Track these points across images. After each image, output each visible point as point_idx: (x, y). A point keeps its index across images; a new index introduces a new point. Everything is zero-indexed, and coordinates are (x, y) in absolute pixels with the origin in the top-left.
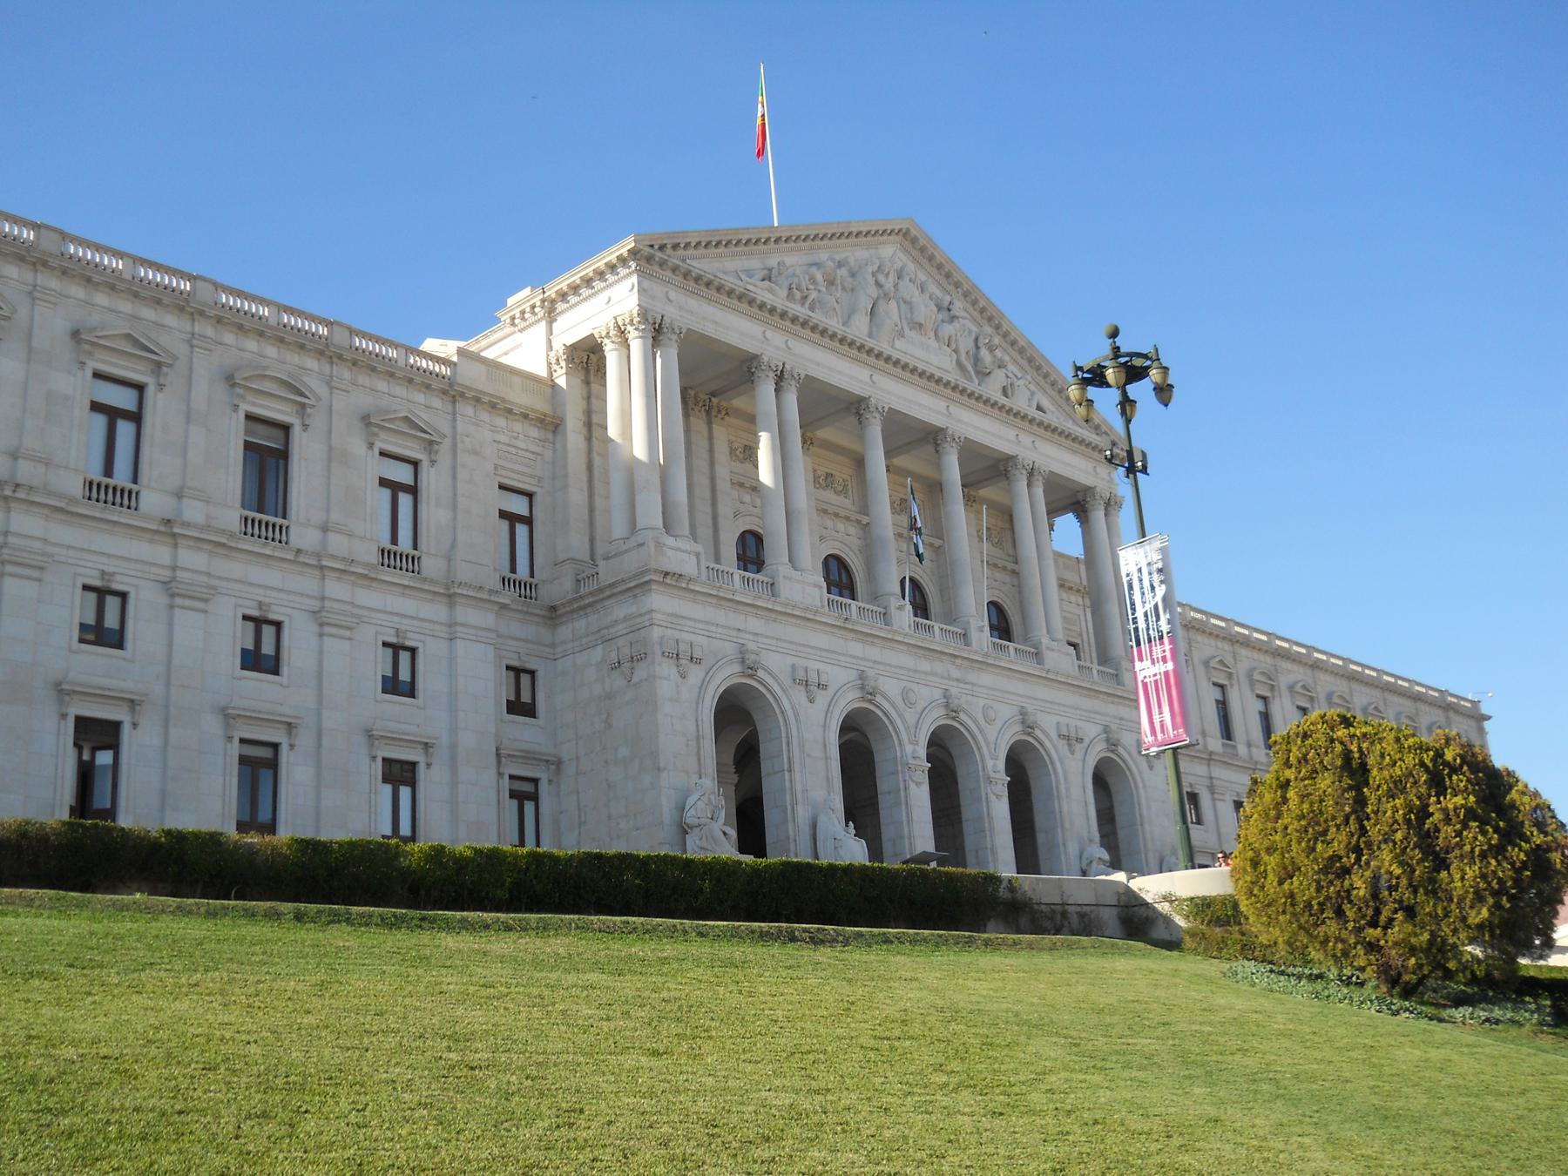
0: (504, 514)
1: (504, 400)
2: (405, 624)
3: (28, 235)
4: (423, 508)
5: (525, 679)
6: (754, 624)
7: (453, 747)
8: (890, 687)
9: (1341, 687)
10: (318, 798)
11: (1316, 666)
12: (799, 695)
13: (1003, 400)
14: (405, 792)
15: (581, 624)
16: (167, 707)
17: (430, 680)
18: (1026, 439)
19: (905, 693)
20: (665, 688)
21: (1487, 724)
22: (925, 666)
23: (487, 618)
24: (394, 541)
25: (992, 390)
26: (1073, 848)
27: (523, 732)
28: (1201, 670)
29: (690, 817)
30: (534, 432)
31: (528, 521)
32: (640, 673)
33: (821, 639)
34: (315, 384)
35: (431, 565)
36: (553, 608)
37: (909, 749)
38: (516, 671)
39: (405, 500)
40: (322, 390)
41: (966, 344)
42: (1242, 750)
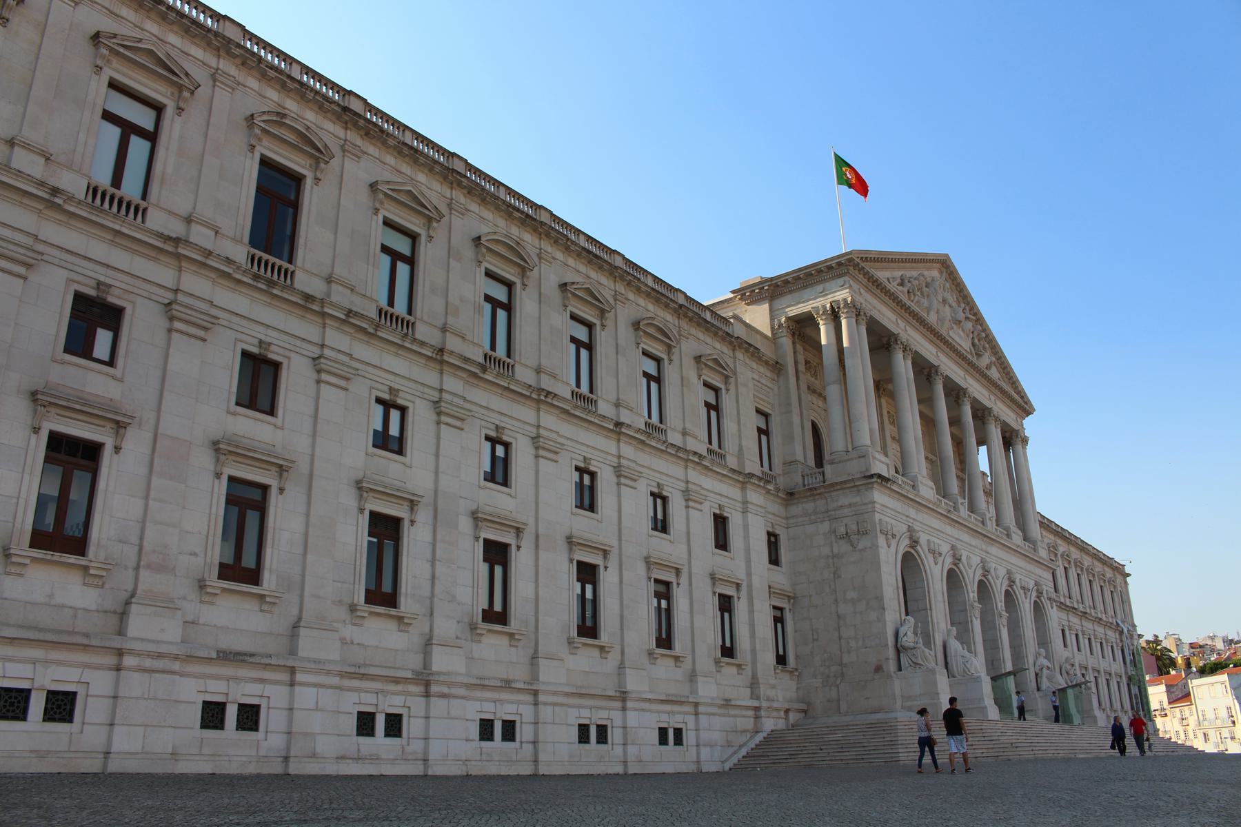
7: (750, 586)
15: (810, 506)
30: (769, 374)
32: (864, 543)
36: (792, 494)
37: (971, 595)
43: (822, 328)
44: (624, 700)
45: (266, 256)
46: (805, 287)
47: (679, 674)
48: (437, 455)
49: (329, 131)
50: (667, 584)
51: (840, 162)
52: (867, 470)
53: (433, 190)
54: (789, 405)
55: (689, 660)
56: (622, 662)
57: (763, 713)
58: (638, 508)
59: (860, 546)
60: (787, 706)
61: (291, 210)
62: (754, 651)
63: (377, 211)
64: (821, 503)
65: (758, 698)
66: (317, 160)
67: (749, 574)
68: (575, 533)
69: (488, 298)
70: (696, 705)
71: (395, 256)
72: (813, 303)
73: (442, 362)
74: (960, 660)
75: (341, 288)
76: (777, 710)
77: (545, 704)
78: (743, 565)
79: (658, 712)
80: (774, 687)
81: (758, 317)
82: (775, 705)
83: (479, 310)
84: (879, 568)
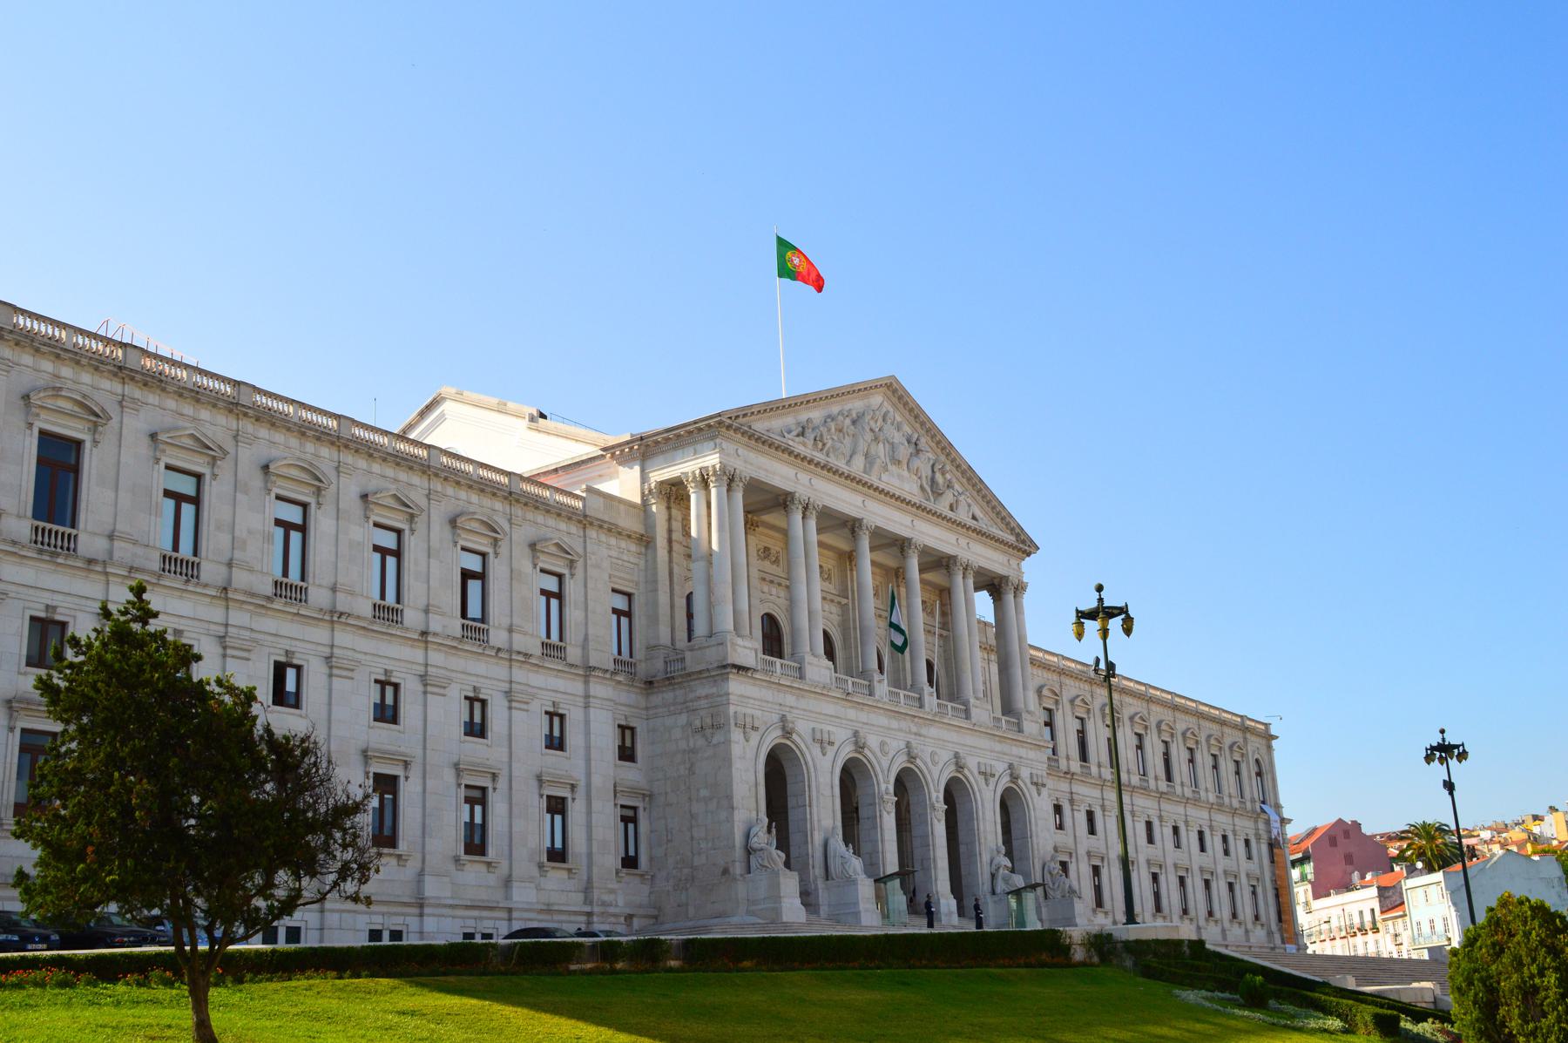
0: (615, 611)
1: (617, 526)
2: (558, 698)
3: (332, 424)
4: (567, 611)
5: (628, 733)
6: (790, 700)
7: (589, 785)
9: (1167, 715)
10: (511, 826)
11: (1151, 700)
13: (950, 514)
14: (558, 818)
15: (669, 696)
16: (424, 765)
17: (574, 738)
18: (963, 541)
19: (882, 744)
20: (736, 750)
21: (1274, 743)
22: (895, 724)
24: (548, 636)
25: (942, 507)
26: (986, 858)
27: (631, 774)
28: (1068, 706)
30: (633, 547)
32: (718, 737)
33: (829, 708)
35: (573, 654)
36: (651, 683)
37: (883, 787)
38: (622, 728)
40: (506, 527)
41: (926, 471)
42: (1094, 770)
43: (693, 498)
44: (421, 906)
45: (48, 526)
46: (675, 449)
47: (492, 879)
49: (105, 389)
50: (484, 790)
51: (783, 245)
52: (725, 658)
53: (216, 425)
54: (656, 582)
55: (505, 864)
56: (423, 869)
57: (595, 919)
58: (449, 713)
59: (715, 741)
60: (628, 911)
61: (72, 475)
62: (590, 855)
63: (157, 461)
64: (680, 693)
65: (591, 903)
66: (96, 424)
67: (589, 775)
68: (372, 745)
69: (279, 522)
70: (510, 910)
71: (179, 498)
72: (686, 466)
73: (227, 599)
74: (839, 861)
75: (123, 544)
76: (615, 915)
77: (333, 911)
78: (581, 763)
79: (463, 918)
80: (612, 891)
81: (625, 484)
82: (612, 910)
83: (269, 538)
84: (730, 766)
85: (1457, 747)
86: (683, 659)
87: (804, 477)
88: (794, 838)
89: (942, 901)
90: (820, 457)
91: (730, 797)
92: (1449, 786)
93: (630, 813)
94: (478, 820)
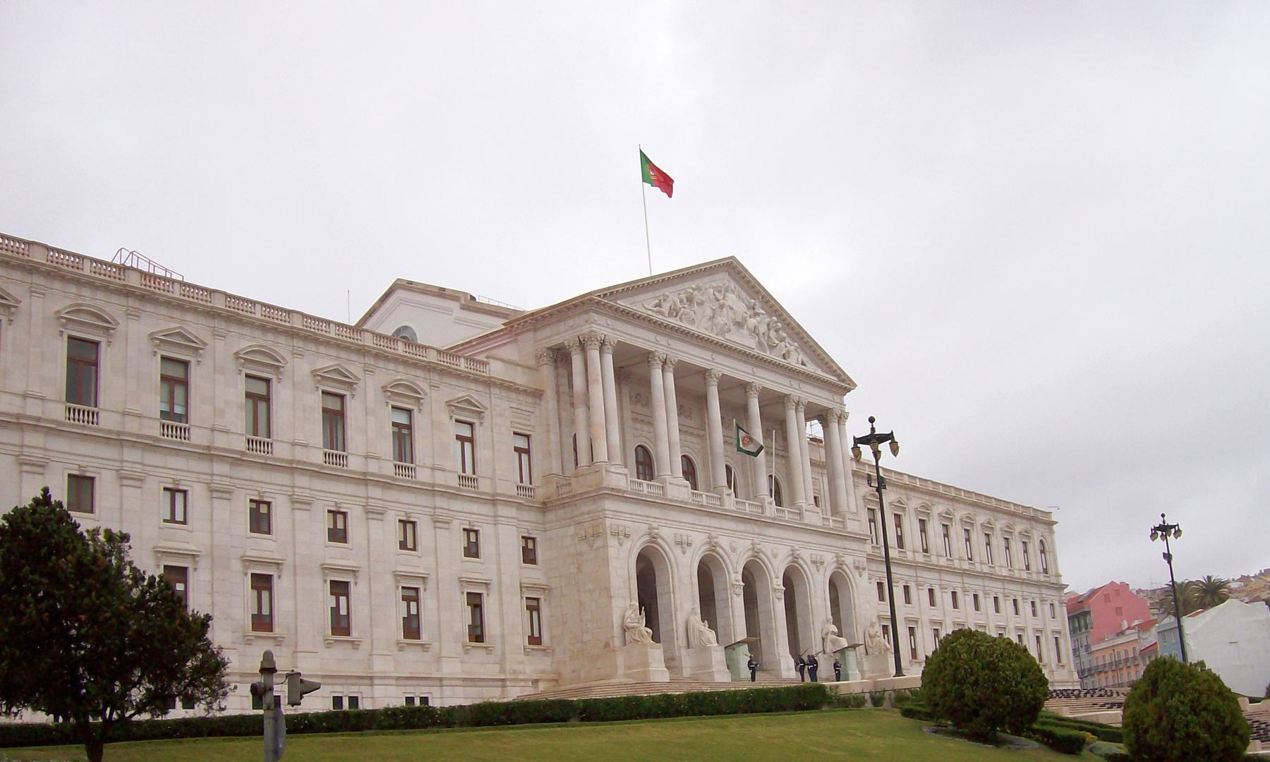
0: (516, 449)
4: (477, 450)
8: (724, 541)
12: (678, 550)
15: (561, 513)
17: (485, 547)
18: (795, 383)
20: (612, 552)
22: (741, 527)
23: (512, 512)
24: (464, 471)
27: (533, 574)
29: (629, 623)
30: (530, 400)
31: (527, 451)
32: (598, 543)
34: (423, 385)
37: (733, 576)
39: (468, 446)
48: (212, 520)
57: (508, 683)
58: (389, 532)
62: (503, 636)
65: (505, 672)
74: (697, 633)
80: (522, 663)
82: (521, 677)
85: (1174, 527)
86: (570, 484)
87: (663, 340)
88: (662, 618)
89: (782, 661)
90: (673, 321)
91: (608, 589)
92: (1168, 557)
93: (534, 603)
94: (413, 612)
